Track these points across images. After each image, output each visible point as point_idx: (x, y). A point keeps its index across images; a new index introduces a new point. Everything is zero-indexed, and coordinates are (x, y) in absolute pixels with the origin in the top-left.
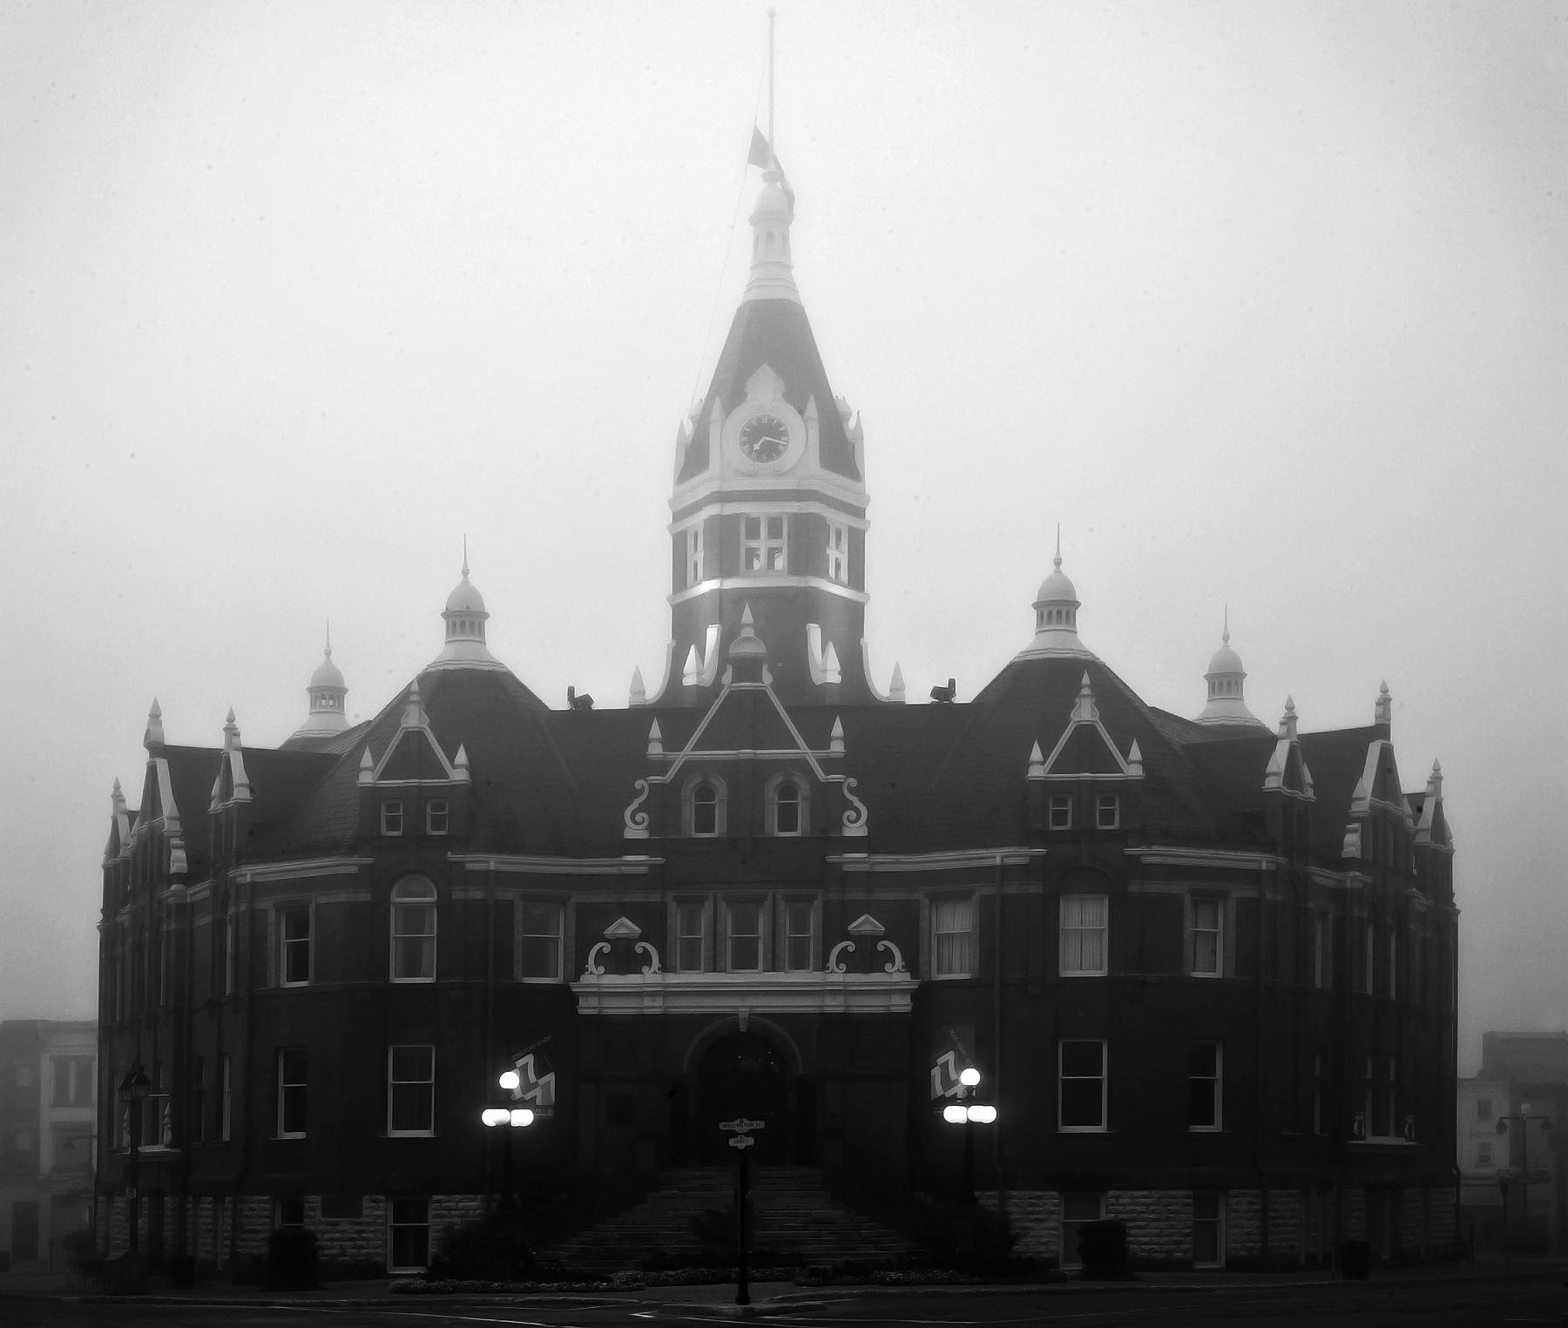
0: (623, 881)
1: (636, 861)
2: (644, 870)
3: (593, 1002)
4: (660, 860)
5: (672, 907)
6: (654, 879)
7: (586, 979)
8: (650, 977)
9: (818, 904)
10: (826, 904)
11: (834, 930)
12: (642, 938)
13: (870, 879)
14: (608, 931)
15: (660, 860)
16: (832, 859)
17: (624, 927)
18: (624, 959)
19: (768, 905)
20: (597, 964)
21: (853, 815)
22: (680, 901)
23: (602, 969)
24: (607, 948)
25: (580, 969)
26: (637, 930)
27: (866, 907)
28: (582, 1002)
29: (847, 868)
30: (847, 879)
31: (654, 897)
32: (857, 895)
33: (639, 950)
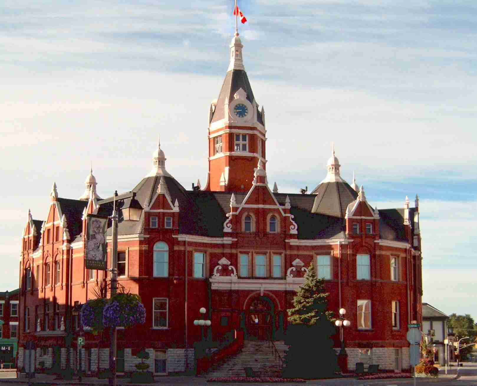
0: (223, 246)
1: (228, 240)
2: (230, 242)
3: (216, 285)
4: (236, 240)
5: (239, 255)
6: (234, 245)
7: (213, 277)
8: (234, 277)
9: (283, 255)
10: (286, 255)
11: (288, 263)
12: (231, 265)
13: (298, 248)
14: (220, 262)
15: (236, 240)
16: (287, 241)
17: (224, 261)
18: (225, 271)
19: (268, 254)
20: (217, 273)
21: (293, 227)
22: (241, 252)
23: (218, 274)
24: (220, 268)
25: (211, 274)
26: (229, 263)
27: (298, 256)
28: (212, 285)
29: (291, 244)
30: (291, 247)
31: (234, 251)
32: (295, 252)
33: (230, 269)
